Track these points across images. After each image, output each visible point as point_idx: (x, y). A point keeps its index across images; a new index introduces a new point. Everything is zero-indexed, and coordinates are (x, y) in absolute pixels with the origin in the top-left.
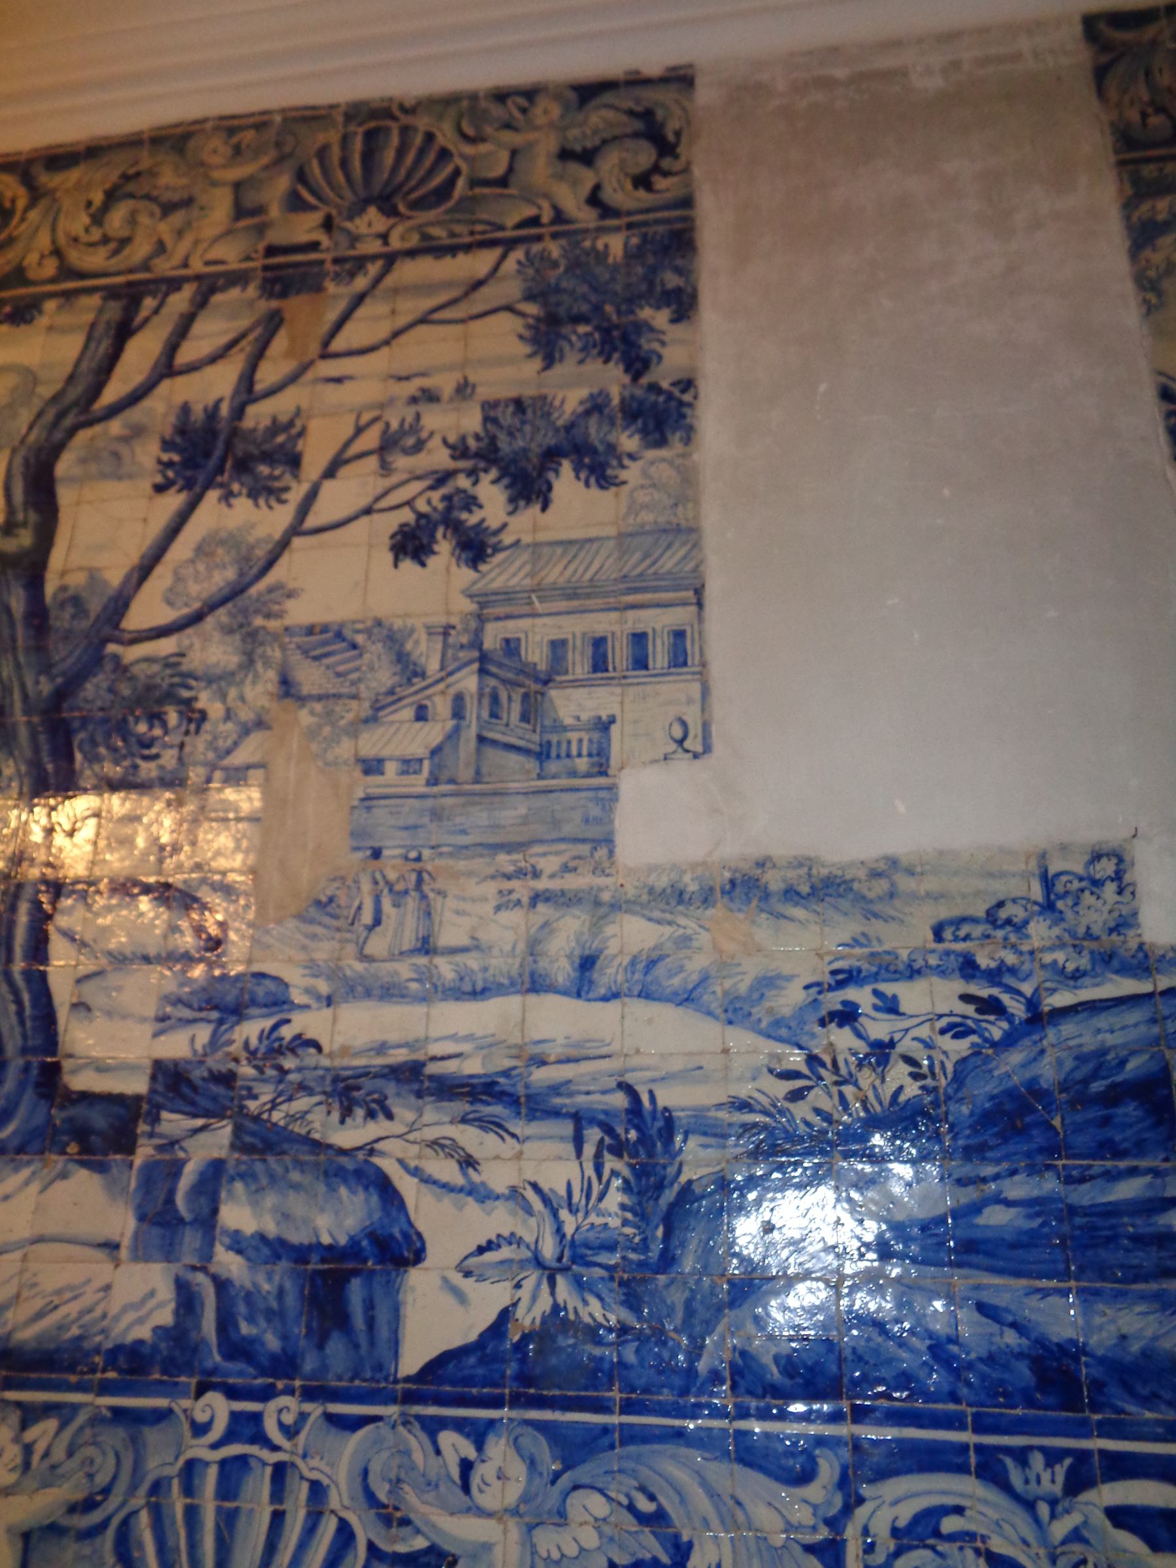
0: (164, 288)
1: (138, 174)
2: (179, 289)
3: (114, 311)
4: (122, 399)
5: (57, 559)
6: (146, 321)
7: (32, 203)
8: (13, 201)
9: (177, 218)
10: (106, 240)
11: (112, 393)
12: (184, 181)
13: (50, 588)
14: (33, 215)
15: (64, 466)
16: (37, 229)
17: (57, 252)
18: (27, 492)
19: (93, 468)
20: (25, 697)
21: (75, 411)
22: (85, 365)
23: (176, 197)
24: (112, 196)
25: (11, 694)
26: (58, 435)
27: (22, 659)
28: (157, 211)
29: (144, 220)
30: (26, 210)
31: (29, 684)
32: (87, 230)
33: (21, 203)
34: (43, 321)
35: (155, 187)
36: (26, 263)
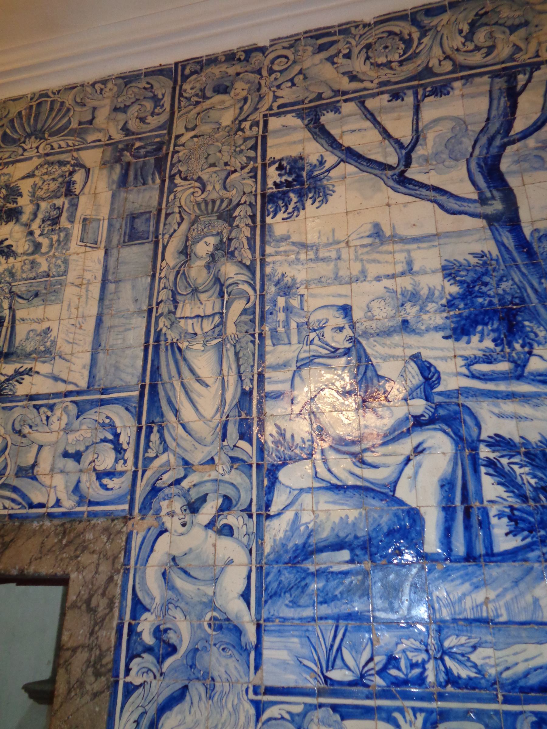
0: (528, 69)
1: (486, 13)
2: (538, 68)
3: (500, 83)
4: (528, 129)
5: (524, 215)
6: (525, 86)
7: (423, 35)
8: (410, 35)
9: (522, 32)
10: (478, 48)
11: (519, 126)
12: (518, 13)
13: (527, 231)
14: (425, 40)
15: (505, 165)
16: (431, 47)
17: (447, 57)
18: (486, 182)
19: (526, 165)
20: (536, 291)
21: (499, 137)
22: (494, 113)
23: (517, 22)
24: (474, 26)
25: (526, 291)
26: (494, 151)
27: (524, 270)
28: (507, 31)
29: (499, 36)
30: (420, 39)
31: (536, 285)
32: (464, 44)
33: (416, 35)
34: (457, 92)
35: (500, 18)
36: (430, 65)
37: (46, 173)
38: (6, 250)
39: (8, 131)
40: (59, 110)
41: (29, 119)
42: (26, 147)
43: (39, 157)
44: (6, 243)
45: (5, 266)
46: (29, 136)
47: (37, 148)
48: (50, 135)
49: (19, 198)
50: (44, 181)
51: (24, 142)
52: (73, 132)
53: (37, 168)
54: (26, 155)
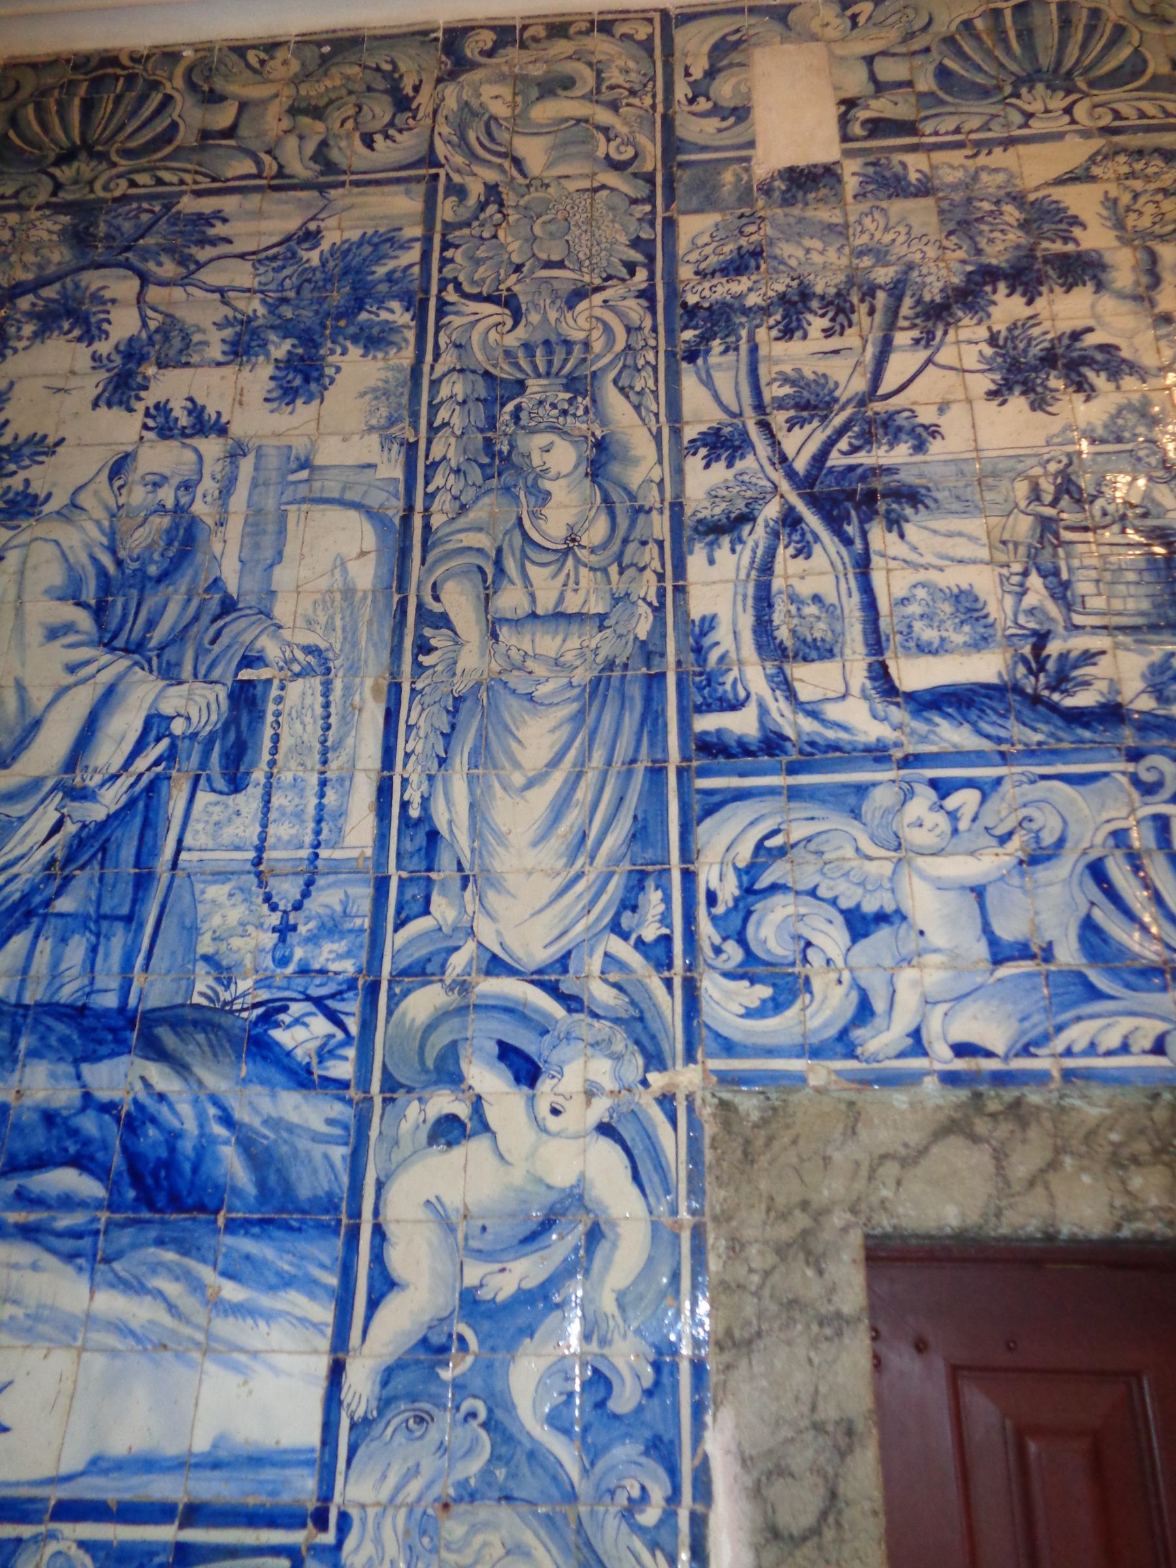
37: (1132, 175)
38: (1099, 357)
39: (949, 63)
40: (1091, 30)
41: (1005, 41)
42: (1029, 108)
43: (1086, 134)
44: (1090, 340)
45: (1116, 399)
46: (1029, 80)
47: (1068, 110)
48: (1092, 84)
49: (1077, 232)
50: (1136, 196)
51: (1018, 96)
52: (1156, 83)
53: (1092, 159)
54: (1038, 126)
